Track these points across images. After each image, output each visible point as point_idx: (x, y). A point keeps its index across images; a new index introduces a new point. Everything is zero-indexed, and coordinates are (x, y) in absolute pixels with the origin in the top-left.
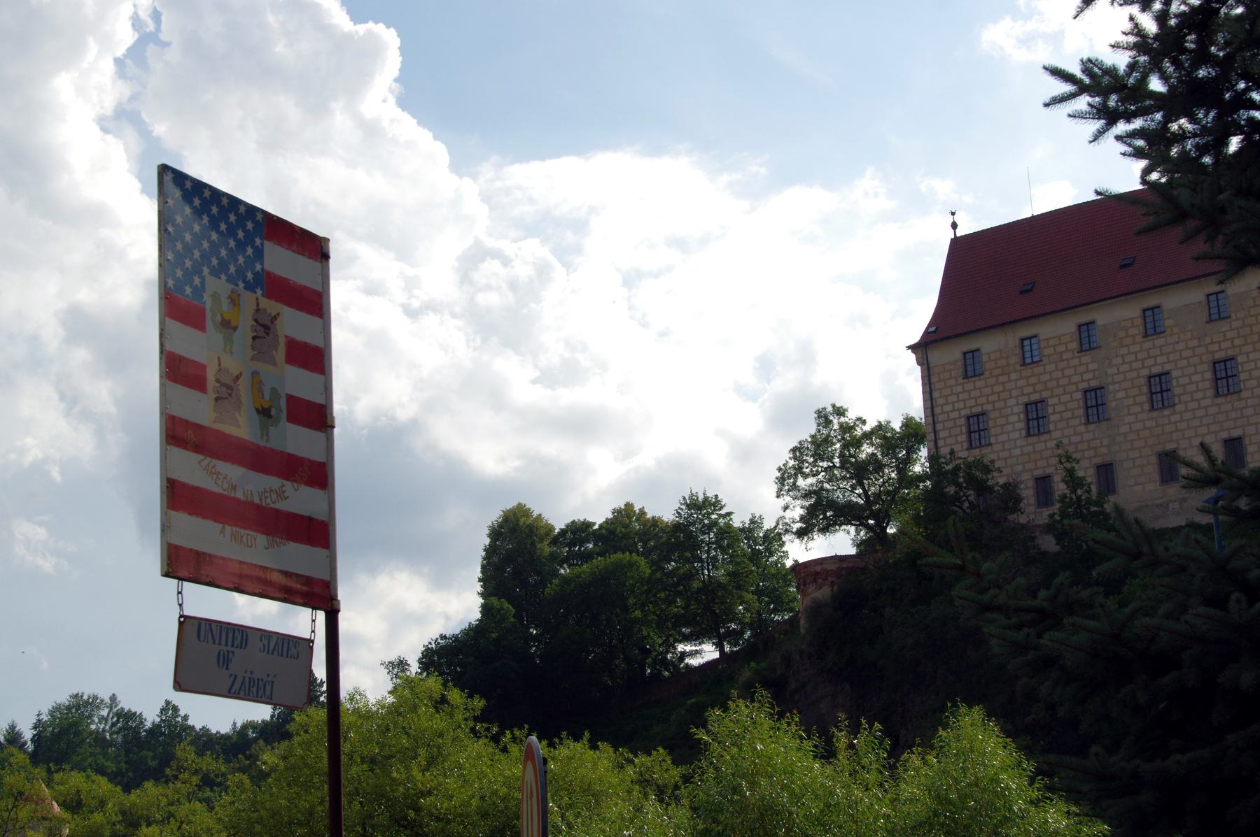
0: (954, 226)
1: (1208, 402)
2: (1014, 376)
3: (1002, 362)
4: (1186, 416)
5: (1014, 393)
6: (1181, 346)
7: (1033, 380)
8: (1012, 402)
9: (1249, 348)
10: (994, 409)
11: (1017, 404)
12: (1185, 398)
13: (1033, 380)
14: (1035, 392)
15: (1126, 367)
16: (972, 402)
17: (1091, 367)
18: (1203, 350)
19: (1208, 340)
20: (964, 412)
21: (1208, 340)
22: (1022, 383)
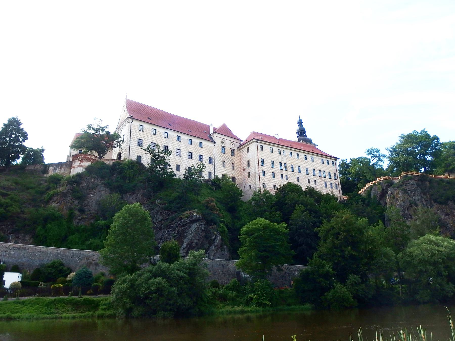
0: (127, 96)
1: (187, 159)
2: (150, 135)
3: (148, 131)
4: (182, 159)
5: (150, 139)
6: (183, 146)
7: (154, 138)
8: (149, 140)
9: (195, 152)
10: (145, 140)
11: (150, 141)
12: (183, 156)
13: (154, 138)
14: (154, 141)
15: (173, 145)
16: (140, 136)
17: (166, 141)
18: (187, 148)
19: (188, 147)
20: (137, 137)
21: (188, 147)
22: (151, 137)
